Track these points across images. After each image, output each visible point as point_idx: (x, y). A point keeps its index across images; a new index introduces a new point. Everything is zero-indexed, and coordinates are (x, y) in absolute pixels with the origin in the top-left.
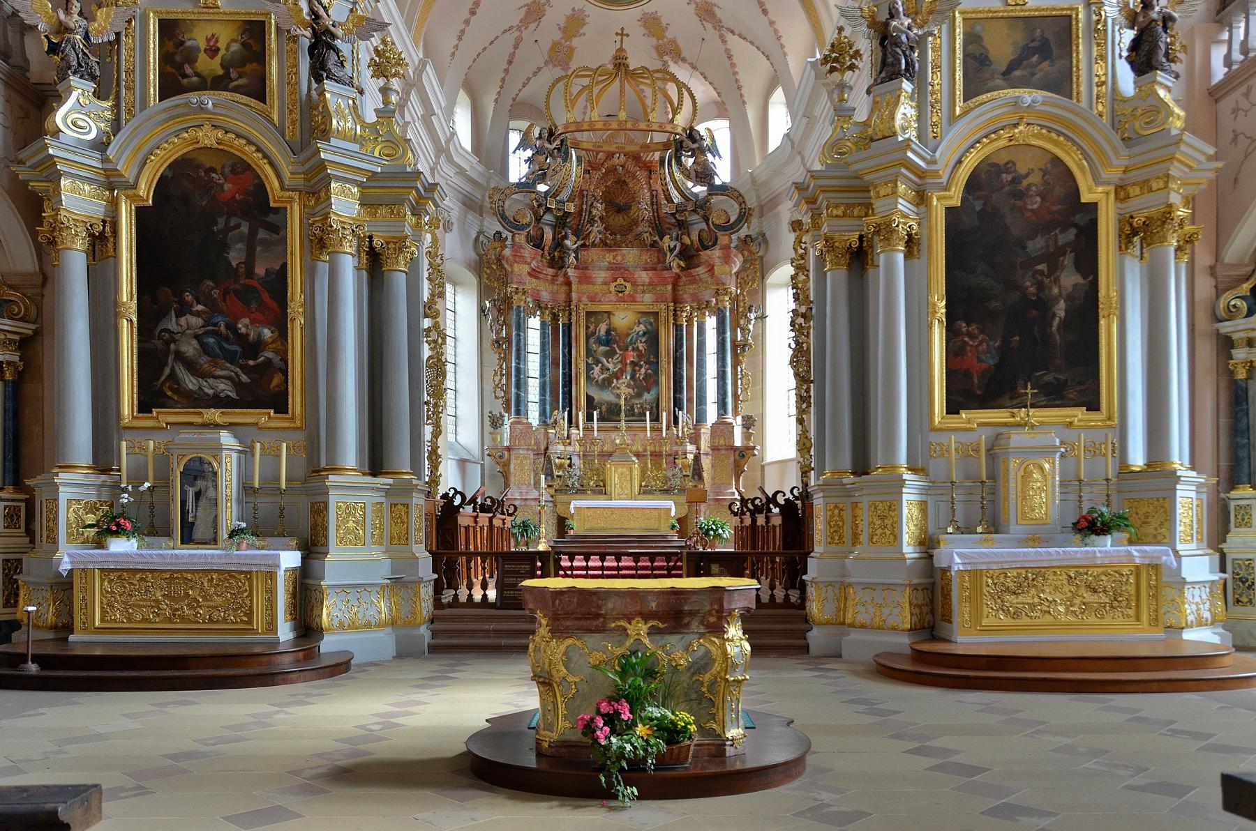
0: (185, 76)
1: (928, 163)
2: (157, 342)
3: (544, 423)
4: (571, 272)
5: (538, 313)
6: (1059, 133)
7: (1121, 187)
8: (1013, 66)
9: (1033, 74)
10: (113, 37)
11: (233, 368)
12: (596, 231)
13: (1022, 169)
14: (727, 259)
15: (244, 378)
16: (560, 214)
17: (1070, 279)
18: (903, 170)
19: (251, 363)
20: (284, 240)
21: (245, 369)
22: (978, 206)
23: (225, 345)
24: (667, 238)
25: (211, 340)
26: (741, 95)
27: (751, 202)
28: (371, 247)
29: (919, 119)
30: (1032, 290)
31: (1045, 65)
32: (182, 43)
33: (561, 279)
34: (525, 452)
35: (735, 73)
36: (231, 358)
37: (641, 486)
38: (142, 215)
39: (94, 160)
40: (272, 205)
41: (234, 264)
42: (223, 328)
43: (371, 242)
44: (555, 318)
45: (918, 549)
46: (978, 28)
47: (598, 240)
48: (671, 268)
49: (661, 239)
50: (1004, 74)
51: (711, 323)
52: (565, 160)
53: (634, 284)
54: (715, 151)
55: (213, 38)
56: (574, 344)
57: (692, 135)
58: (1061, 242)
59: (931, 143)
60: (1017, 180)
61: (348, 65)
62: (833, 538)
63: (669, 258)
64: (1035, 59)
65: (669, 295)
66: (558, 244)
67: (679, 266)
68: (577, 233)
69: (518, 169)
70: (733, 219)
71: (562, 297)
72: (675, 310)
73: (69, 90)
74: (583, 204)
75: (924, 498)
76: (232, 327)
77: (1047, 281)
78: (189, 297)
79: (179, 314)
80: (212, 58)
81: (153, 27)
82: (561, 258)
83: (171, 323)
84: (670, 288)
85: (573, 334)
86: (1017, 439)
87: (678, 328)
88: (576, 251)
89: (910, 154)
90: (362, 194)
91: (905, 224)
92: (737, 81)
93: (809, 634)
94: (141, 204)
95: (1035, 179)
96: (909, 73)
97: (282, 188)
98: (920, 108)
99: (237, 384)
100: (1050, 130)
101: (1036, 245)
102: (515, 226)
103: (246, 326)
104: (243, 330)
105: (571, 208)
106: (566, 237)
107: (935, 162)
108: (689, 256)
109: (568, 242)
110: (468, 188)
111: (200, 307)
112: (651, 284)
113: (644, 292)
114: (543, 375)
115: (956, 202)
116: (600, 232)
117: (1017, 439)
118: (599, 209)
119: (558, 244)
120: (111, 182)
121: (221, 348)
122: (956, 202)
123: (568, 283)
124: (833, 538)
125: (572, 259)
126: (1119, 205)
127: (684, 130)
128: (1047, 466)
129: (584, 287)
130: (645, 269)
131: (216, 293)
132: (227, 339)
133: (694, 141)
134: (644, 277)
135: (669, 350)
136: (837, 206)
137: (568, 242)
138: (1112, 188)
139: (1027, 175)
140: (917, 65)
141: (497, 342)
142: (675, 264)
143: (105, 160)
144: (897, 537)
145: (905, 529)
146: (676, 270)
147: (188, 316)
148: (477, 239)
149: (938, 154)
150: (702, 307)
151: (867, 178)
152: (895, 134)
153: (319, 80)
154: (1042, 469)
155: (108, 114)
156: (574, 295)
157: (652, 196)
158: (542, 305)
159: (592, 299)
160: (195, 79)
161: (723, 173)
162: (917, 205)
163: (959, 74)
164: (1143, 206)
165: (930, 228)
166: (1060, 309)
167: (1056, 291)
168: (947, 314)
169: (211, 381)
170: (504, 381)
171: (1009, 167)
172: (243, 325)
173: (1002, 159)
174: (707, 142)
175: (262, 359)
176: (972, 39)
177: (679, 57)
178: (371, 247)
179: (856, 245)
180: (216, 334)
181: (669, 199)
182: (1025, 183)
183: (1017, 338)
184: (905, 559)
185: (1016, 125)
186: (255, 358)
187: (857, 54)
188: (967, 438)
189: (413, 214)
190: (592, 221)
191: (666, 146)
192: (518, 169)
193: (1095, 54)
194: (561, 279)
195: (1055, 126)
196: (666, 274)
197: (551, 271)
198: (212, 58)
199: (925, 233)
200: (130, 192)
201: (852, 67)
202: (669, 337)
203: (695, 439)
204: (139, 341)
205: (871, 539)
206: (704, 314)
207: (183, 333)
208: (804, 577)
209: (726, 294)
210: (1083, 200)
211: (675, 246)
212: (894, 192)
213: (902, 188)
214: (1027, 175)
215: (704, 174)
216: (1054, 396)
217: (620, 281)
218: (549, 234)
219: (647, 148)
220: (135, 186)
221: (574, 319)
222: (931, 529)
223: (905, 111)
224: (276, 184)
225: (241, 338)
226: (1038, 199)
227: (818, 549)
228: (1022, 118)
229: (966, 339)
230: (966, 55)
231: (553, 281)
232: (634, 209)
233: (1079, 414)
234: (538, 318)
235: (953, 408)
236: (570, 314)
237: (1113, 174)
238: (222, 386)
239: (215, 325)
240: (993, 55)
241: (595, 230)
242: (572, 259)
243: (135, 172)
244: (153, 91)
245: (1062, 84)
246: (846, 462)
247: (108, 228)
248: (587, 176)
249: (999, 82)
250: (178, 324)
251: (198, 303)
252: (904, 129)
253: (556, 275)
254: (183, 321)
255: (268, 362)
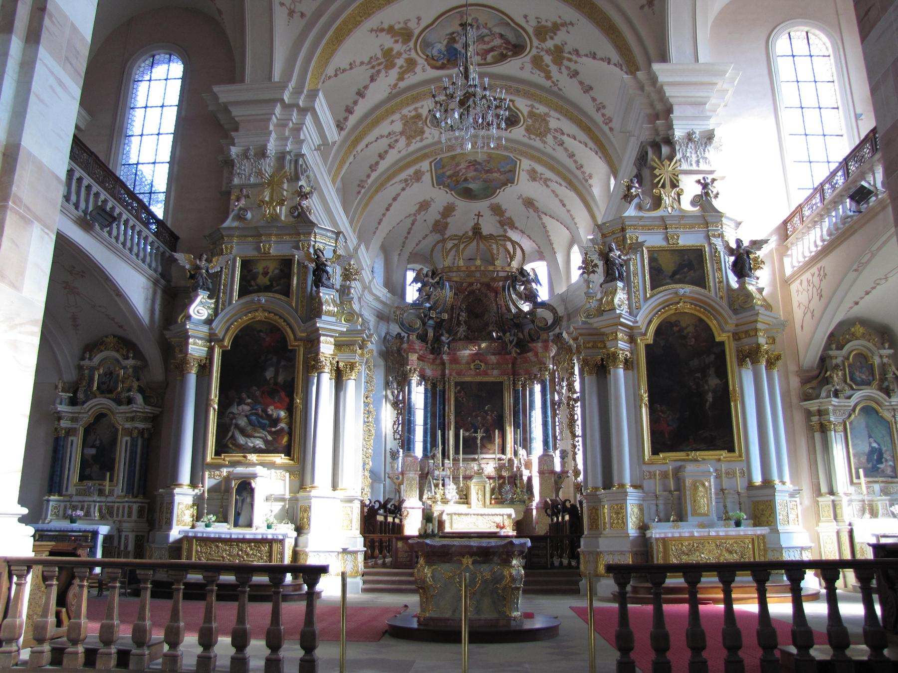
0: (251, 286)
1: (634, 322)
2: (226, 419)
3: (425, 455)
4: (445, 357)
5: (423, 383)
6: (701, 307)
7: (736, 333)
8: (674, 273)
9: (685, 277)
10: (219, 269)
11: (264, 432)
12: (462, 330)
13: (683, 324)
14: (546, 348)
15: (269, 438)
16: (438, 320)
17: (713, 381)
18: (620, 327)
19: (273, 429)
20: (294, 366)
21: (270, 433)
22: (662, 343)
23: (261, 420)
24: (508, 334)
25: (254, 418)
26: (553, 248)
27: (561, 311)
28: (338, 367)
29: (629, 299)
30: (694, 387)
31: (691, 273)
32: (251, 271)
33: (438, 361)
34: (413, 475)
35: (548, 236)
36: (263, 427)
37: (491, 498)
38: (225, 355)
39: (205, 329)
40: (290, 348)
41: (268, 378)
42: (260, 411)
43: (338, 365)
44: (434, 386)
45: (638, 531)
46: (656, 255)
47: (463, 336)
48: (510, 353)
49: (504, 334)
50: (670, 277)
51: (537, 388)
52: (442, 289)
53: (486, 363)
54: (537, 281)
55: (267, 267)
56: (447, 403)
57: (522, 272)
58: (707, 362)
59: (635, 311)
60: (682, 330)
61: (331, 279)
62: (592, 526)
63: (509, 347)
64: (686, 270)
65: (510, 371)
66: (437, 339)
67: (516, 352)
68: (449, 332)
69: (412, 294)
70: (550, 322)
71: (439, 372)
72: (514, 380)
73: (197, 296)
74: (453, 314)
75: (641, 502)
76: (265, 411)
77: (701, 382)
78: (244, 395)
79: (238, 405)
80: (265, 277)
81: (238, 264)
82: (439, 348)
83: (234, 409)
84: (510, 366)
85: (447, 397)
86: (690, 468)
87: (516, 392)
88: (449, 344)
89: (622, 320)
90: (335, 341)
91: (623, 354)
92: (550, 240)
93: (580, 583)
94: (225, 349)
95: (691, 329)
96: (621, 278)
97: (296, 339)
98: (629, 293)
99: (266, 441)
100: (696, 305)
101: (694, 363)
102: (409, 329)
103: (272, 410)
104: (270, 412)
105: (445, 316)
106: (442, 335)
107: (637, 322)
108: (522, 346)
109: (443, 338)
110: (379, 306)
111: (249, 401)
112: (498, 363)
113: (493, 369)
114: (425, 424)
115: (650, 341)
116: (464, 331)
117: (690, 468)
118: (464, 316)
119: (437, 339)
120: (212, 339)
121: (259, 422)
122: (650, 341)
123: (443, 364)
124: (592, 526)
125: (446, 348)
126: (736, 342)
127: (517, 269)
128: (707, 484)
129: (454, 366)
130: (494, 354)
131: (258, 393)
132: (262, 417)
133: (524, 276)
134: (493, 359)
135: (510, 406)
136: (588, 343)
137: (443, 338)
138: (730, 334)
139: (687, 327)
140: (625, 274)
141: (396, 403)
142: (514, 352)
143: (211, 329)
144: (625, 524)
145: (629, 520)
146: (514, 354)
147: (243, 405)
148: (385, 337)
149: (638, 318)
150: (532, 378)
151: (603, 330)
152: (614, 309)
153: (317, 287)
154: (704, 485)
155: (213, 306)
156: (447, 371)
157: (498, 307)
158: (426, 378)
159: (459, 373)
160: (256, 287)
161: (543, 295)
162: (630, 343)
163: (647, 277)
164: (747, 342)
165: (638, 355)
166: (710, 397)
167: (706, 387)
168: (650, 401)
169: (252, 439)
170: (400, 428)
171: (677, 323)
172: (270, 410)
173: (673, 319)
174: (532, 275)
175: (279, 427)
176: (651, 260)
177: (513, 226)
178: (338, 367)
179: (599, 363)
180: (256, 414)
181: (510, 310)
182: (685, 332)
183: (687, 413)
184: (629, 537)
185: (678, 303)
186: (275, 427)
187: (596, 266)
188: (664, 468)
189: (360, 349)
190: (459, 324)
191: (506, 278)
192: (412, 294)
193: (715, 267)
194: (438, 361)
195: (696, 302)
196: (508, 357)
197: (431, 356)
198: (265, 277)
199: (635, 357)
200: (220, 343)
201: (594, 272)
202: (510, 398)
203: (528, 465)
204: (218, 418)
205: (611, 526)
206: (533, 382)
207: (239, 414)
208: (579, 550)
209: (546, 371)
210: (717, 340)
211: (513, 340)
212: (616, 339)
213: (620, 335)
214: (687, 327)
215: (531, 296)
216: (711, 444)
217: (477, 362)
218: (431, 334)
219: (494, 279)
220: (223, 340)
221: (447, 387)
222: (646, 521)
223: (621, 296)
224: (292, 337)
225: (269, 417)
226: (693, 340)
227: (586, 533)
228: (681, 299)
229: (660, 414)
230: (651, 268)
231: (433, 363)
232: (486, 316)
233: (724, 454)
234: (423, 386)
235: (655, 451)
236: (444, 384)
237: (731, 326)
238: (258, 442)
239: (256, 410)
240: (664, 267)
241: (461, 330)
242: (446, 348)
243: (223, 333)
244: (236, 294)
245: (701, 281)
246: (600, 484)
247: (208, 362)
248: (456, 297)
249: (668, 281)
250: (238, 409)
251: (249, 398)
252: (620, 306)
253: (435, 359)
254: (240, 408)
255: (282, 429)
